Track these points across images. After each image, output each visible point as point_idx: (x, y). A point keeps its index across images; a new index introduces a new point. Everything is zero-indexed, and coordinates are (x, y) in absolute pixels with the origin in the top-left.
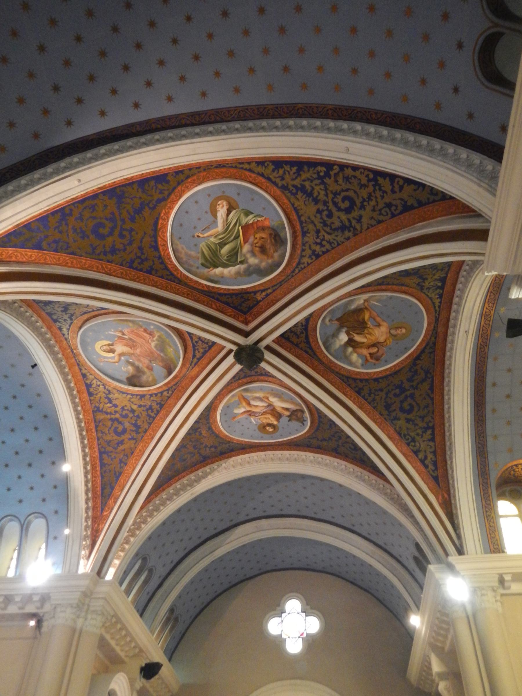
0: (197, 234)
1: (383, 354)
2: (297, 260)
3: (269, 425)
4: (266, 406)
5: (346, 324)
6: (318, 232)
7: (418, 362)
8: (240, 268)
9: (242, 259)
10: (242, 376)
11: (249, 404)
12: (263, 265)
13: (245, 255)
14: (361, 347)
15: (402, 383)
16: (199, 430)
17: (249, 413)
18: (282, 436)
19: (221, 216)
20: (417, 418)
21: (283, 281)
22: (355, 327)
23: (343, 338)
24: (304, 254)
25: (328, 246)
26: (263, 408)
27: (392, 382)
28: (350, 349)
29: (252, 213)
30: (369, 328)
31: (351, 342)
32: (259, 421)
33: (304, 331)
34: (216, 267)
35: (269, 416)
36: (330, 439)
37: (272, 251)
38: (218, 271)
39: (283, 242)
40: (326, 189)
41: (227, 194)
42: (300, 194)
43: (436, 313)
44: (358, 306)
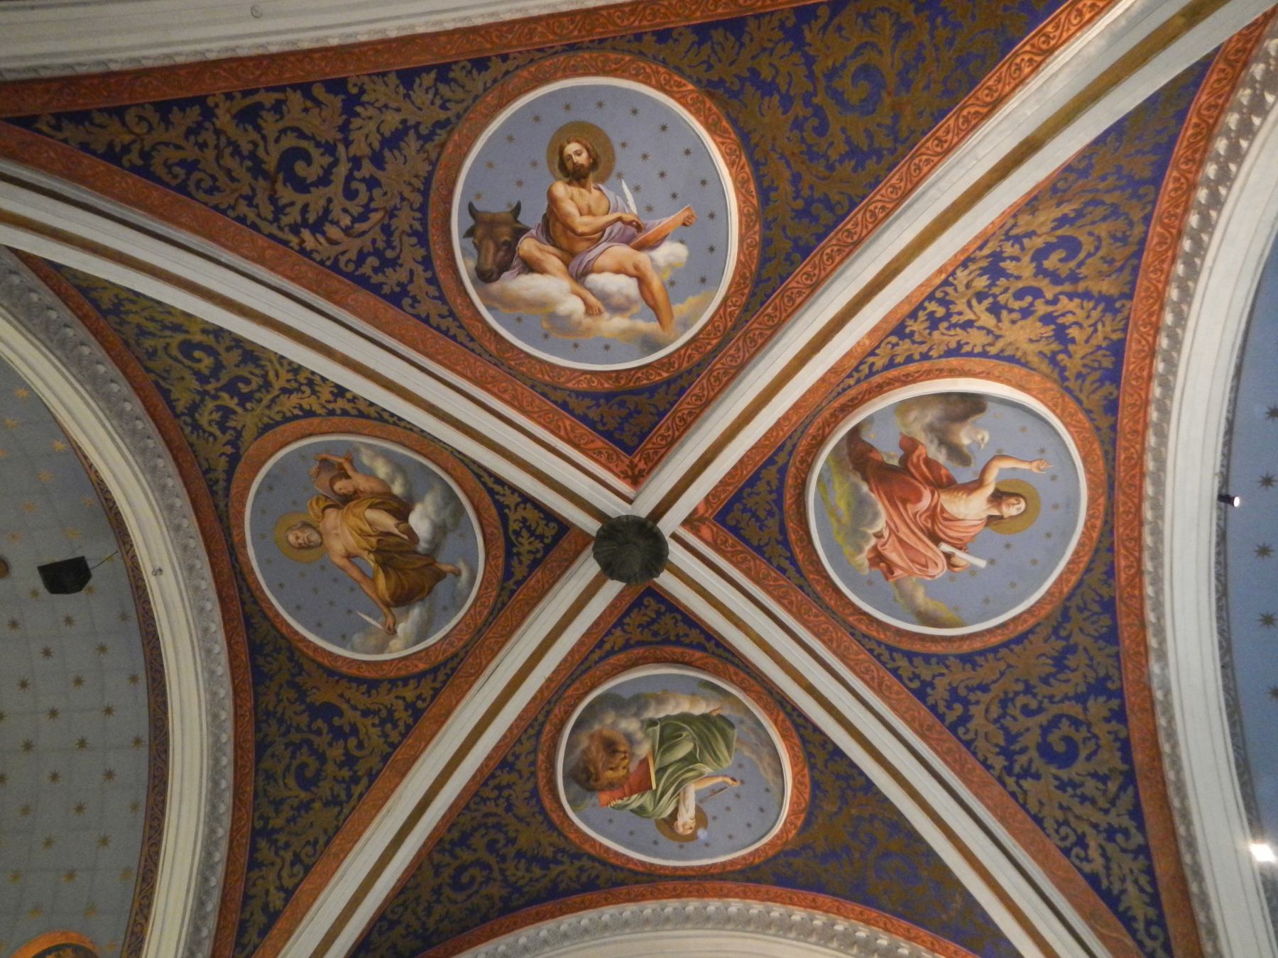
0: (737, 785)
1: (319, 473)
2: (543, 738)
3: (576, 176)
4: (592, 271)
5: (419, 564)
6: (509, 808)
7: (229, 450)
8: (658, 712)
9: (650, 729)
10: (662, 390)
11: (642, 281)
12: (609, 718)
13: (647, 735)
14: (373, 494)
15: (241, 404)
16: (799, 204)
17: (641, 237)
18: (534, 115)
19: (687, 811)
20: (159, 333)
21: (569, 686)
22: (401, 553)
23: (421, 522)
24: (531, 758)
25: (487, 792)
26: (603, 261)
27: (269, 407)
28: (397, 489)
29: (632, 811)
30: (370, 552)
31: (401, 510)
32: (610, 195)
33: (513, 538)
34: (705, 717)
35: (583, 223)
36: (378, 160)
37: (593, 748)
38: (700, 709)
39: (570, 776)
40: (505, 880)
41: (675, 845)
42: (549, 852)
43: (241, 573)
44: (407, 612)
